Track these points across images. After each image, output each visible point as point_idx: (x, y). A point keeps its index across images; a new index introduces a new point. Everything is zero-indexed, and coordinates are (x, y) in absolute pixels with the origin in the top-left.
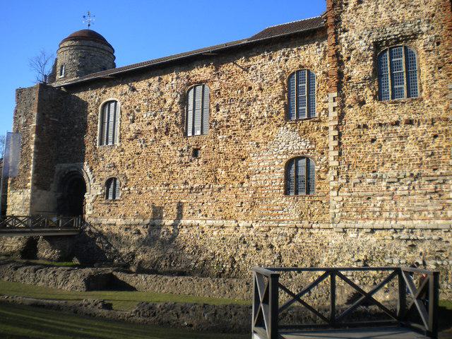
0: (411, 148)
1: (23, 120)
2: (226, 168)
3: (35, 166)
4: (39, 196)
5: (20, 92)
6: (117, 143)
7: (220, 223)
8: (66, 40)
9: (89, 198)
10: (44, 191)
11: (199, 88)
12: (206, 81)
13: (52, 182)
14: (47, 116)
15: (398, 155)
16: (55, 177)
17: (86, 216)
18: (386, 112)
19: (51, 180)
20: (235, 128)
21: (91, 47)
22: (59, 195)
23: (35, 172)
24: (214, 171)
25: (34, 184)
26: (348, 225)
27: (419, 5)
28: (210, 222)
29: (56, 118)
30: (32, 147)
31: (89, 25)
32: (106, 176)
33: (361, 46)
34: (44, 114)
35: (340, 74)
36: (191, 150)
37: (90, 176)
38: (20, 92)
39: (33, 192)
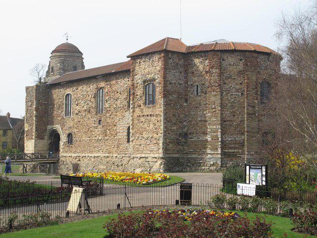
0: (152, 126)
1: (30, 104)
2: (109, 130)
3: (36, 128)
5: (27, 88)
6: (72, 116)
8: (53, 52)
9: (61, 143)
11: (101, 90)
12: (103, 87)
17: (60, 152)
18: (147, 111)
21: (68, 55)
22: (49, 142)
23: (36, 131)
24: (105, 131)
28: (104, 155)
30: (34, 118)
32: (68, 132)
33: (139, 81)
37: (61, 132)
38: (27, 88)
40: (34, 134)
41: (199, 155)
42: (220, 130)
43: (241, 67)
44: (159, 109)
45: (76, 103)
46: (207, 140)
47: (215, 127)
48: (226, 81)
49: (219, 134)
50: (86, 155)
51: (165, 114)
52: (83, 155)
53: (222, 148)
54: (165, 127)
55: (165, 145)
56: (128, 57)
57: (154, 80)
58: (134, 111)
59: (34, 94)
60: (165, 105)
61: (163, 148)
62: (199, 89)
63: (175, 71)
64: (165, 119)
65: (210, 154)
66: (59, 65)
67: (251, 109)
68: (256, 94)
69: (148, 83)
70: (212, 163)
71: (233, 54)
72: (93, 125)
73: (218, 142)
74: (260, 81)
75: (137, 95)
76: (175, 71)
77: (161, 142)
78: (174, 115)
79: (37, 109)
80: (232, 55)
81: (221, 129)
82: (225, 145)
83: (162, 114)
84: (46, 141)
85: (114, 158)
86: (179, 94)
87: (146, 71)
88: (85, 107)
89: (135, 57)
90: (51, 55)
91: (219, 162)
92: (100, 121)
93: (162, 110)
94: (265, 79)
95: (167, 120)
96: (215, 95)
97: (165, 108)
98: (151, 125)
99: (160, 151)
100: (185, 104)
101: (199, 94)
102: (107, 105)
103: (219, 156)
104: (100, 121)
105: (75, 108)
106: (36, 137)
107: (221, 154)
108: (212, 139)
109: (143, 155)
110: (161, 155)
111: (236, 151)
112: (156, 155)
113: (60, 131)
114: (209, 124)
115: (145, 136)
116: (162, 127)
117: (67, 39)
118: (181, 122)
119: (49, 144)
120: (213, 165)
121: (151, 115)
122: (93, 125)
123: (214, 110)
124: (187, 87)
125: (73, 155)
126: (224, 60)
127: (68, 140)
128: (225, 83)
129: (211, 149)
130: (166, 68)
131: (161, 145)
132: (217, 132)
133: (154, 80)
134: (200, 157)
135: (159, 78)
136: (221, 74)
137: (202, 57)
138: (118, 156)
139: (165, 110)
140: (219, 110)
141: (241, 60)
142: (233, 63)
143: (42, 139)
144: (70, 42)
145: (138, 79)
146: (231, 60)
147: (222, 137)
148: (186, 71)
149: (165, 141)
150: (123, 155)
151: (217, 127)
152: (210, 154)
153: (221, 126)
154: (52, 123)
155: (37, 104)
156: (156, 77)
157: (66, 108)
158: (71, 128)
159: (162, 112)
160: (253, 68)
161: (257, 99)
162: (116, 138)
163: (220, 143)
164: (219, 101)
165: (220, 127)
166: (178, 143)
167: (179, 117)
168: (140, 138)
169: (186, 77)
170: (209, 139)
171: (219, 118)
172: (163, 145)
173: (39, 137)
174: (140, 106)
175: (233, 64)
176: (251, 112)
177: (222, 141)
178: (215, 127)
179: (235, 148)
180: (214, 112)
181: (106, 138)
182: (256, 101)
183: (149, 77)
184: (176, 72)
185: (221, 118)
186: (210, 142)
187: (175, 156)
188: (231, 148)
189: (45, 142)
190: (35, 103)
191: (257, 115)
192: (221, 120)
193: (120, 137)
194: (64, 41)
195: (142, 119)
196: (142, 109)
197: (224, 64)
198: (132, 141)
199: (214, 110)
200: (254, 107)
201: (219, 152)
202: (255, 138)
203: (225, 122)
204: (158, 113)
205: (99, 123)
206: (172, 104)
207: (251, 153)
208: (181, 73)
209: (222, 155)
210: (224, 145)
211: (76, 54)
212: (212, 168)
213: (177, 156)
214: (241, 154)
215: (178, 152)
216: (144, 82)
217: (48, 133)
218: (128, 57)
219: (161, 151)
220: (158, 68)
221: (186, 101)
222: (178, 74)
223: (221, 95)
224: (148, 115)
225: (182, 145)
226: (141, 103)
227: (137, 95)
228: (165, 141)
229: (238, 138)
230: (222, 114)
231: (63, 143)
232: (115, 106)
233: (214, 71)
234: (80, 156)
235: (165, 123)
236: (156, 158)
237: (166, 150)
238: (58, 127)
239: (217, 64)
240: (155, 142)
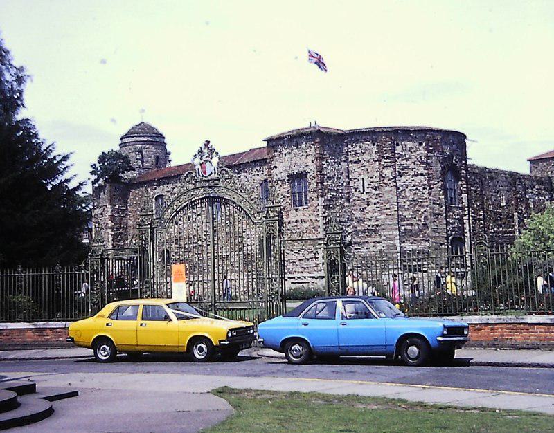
42: (398, 237)
47: (391, 233)
49: (397, 242)
61: (323, 264)
62: (366, 186)
69: (297, 178)
76: (332, 161)
83: (320, 219)
89: (274, 143)
101: (367, 190)
132: (394, 239)
135: (310, 166)
141: (421, 144)
144: (146, 121)
147: (401, 247)
175: (414, 151)
178: (391, 233)
183: (296, 170)
211: (157, 140)
236: (313, 277)
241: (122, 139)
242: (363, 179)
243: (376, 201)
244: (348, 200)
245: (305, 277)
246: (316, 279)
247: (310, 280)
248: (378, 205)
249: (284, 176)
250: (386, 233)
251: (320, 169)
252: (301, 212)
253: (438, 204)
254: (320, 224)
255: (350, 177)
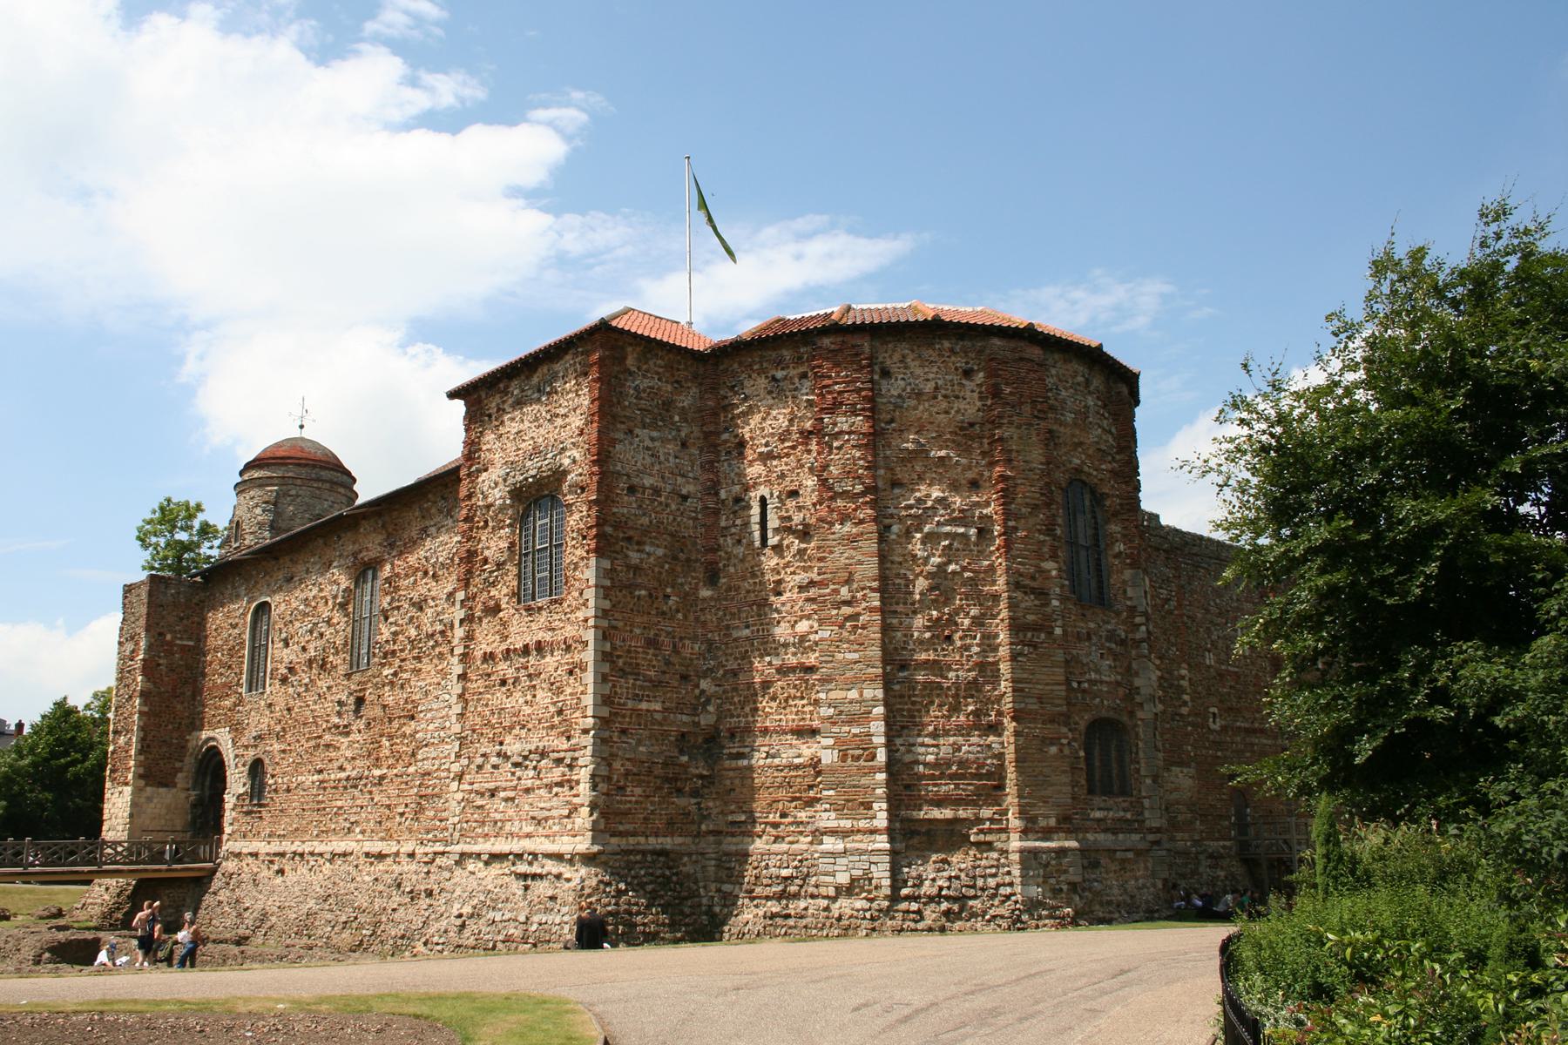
1: (129, 647)
2: (390, 737)
3: (142, 740)
4: (149, 799)
5: (128, 589)
6: (268, 689)
7: (376, 847)
8: (249, 466)
9: (229, 800)
10: (162, 790)
11: (370, 573)
13: (180, 770)
14: (169, 637)
15: (527, 710)
16: (187, 760)
17: (225, 837)
18: (523, 631)
19: (178, 765)
20: (404, 655)
23: (140, 752)
25: (138, 776)
26: (467, 848)
27: (566, 416)
29: (190, 639)
31: (302, 427)
32: (251, 753)
34: (160, 634)
35: (471, 554)
36: (352, 700)
39: (137, 792)
40: (132, 763)
41: (777, 839)
42: (879, 710)
43: (970, 405)
44: (577, 616)
45: (284, 635)
46: (815, 763)
47: (853, 694)
48: (902, 474)
49: (878, 727)
50: (307, 848)
51: (604, 635)
52: (297, 846)
53: (896, 803)
54: (604, 700)
55: (603, 787)
56: (452, 395)
57: (559, 475)
58: (469, 637)
59: (144, 610)
60: (604, 591)
61: (593, 806)
62: (773, 522)
63: (655, 434)
64: (604, 657)
65: (833, 832)
66: (258, 511)
67: (1029, 601)
68: (1049, 531)
69: (536, 496)
70: (843, 879)
71: (931, 345)
72: (336, 720)
73: (874, 770)
74: (1061, 477)
75: (486, 561)
76: (655, 434)
77: (583, 774)
78: (652, 643)
79: (149, 669)
80: (928, 353)
81: (886, 705)
82: (907, 787)
83: (590, 636)
84: (183, 795)
85: (404, 859)
86: (678, 542)
87: (527, 446)
88: (311, 647)
90: (239, 480)
91: (881, 874)
92: (360, 701)
93: (591, 612)
94: (1078, 470)
95: (614, 664)
96: (852, 539)
97: (607, 604)
98: (540, 694)
99: (579, 821)
100: (705, 593)
101: (773, 540)
102: (386, 632)
103: (882, 843)
104: (360, 701)
105: (280, 655)
106: (141, 776)
107: (890, 831)
108: (844, 758)
109: (501, 846)
110: (583, 844)
111: (962, 814)
112: (565, 845)
113: (228, 753)
114: (825, 680)
115: (514, 747)
116: (588, 700)
117: (302, 427)
118: (684, 678)
119: (194, 806)
120: (849, 890)
121: (539, 647)
122: (336, 720)
123: (847, 610)
124: (716, 513)
125: (262, 847)
126: (886, 373)
127: (252, 787)
128: (896, 484)
129: (838, 809)
130: (608, 413)
131: (584, 788)
132: (866, 716)
133: (559, 475)
134: (784, 847)
135: (576, 461)
136: (875, 440)
137: (780, 363)
138: (420, 850)
139: (602, 614)
140: (871, 610)
141: (968, 374)
142: (929, 387)
143: (166, 786)
144: (306, 434)
145: (492, 487)
146: (918, 371)
147: (889, 745)
148: (707, 435)
149: (604, 771)
150: (439, 848)
151: (868, 694)
152: (833, 832)
153: (887, 688)
154: (196, 723)
155: (149, 648)
156: (566, 462)
157: (252, 659)
158: (259, 737)
159: (591, 622)
160: (1027, 409)
161: (1054, 557)
162: (412, 769)
163: (881, 777)
164: (868, 568)
165: (880, 694)
166: (673, 782)
167: (676, 651)
168: (494, 760)
169: (709, 467)
170: (828, 758)
171: (875, 652)
172: (594, 787)
173: (153, 775)
174: (497, 609)
176: (1030, 618)
177: (891, 766)
178: (853, 694)
179: (957, 802)
180: (848, 618)
181: (377, 772)
182: (1049, 565)
183: (532, 467)
184: (664, 441)
185: (884, 649)
186: (832, 770)
187: (654, 842)
188: (939, 803)
189: (175, 799)
190: (143, 644)
191: (1058, 631)
192: (886, 660)
193: (427, 766)
194: (296, 433)
195: (504, 669)
196: (504, 624)
197: (893, 388)
198: (460, 777)
199: (847, 610)
200: (1042, 594)
201: (881, 821)
202: (1053, 750)
203: (903, 667)
204: (570, 631)
205: (357, 711)
206: (639, 587)
207: (1042, 823)
208: (684, 445)
209: (892, 840)
210: (903, 786)
211: (325, 474)
212: (844, 905)
213: (667, 842)
214: (990, 831)
215: (671, 827)
216: (517, 493)
217: (189, 762)
218: (452, 395)
219: (584, 819)
220: (577, 421)
221: (712, 578)
222: (671, 448)
223: (882, 539)
224: (526, 651)
225: (695, 793)
226: (501, 593)
227: (486, 561)
228: (604, 771)
229: (970, 746)
230: (886, 629)
231: (234, 800)
232: (413, 632)
233: (843, 422)
234: (282, 855)
235: (602, 678)
236: (559, 857)
237: (608, 816)
238: (223, 738)
239: (858, 391)
240: (557, 774)
241: (241, 474)
242: (763, 501)
243: (802, 578)
244: (712, 578)
245: (535, 855)
246: (571, 862)
247: (551, 867)
248: (813, 592)
249: (498, 496)
250: (833, 695)
251: (603, 456)
252: (543, 618)
253: (1033, 591)
254: (589, 656)
255: (723, 494)
